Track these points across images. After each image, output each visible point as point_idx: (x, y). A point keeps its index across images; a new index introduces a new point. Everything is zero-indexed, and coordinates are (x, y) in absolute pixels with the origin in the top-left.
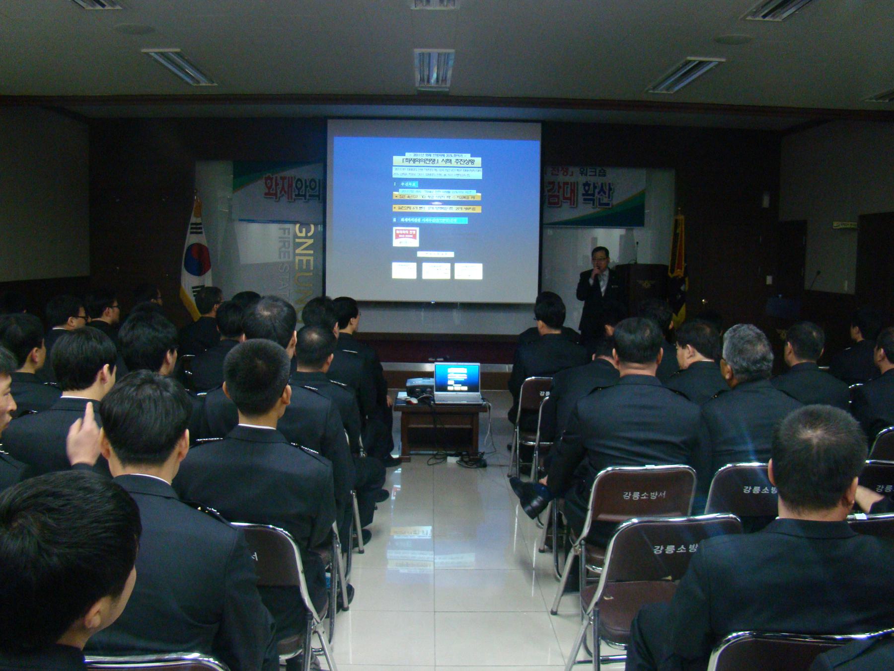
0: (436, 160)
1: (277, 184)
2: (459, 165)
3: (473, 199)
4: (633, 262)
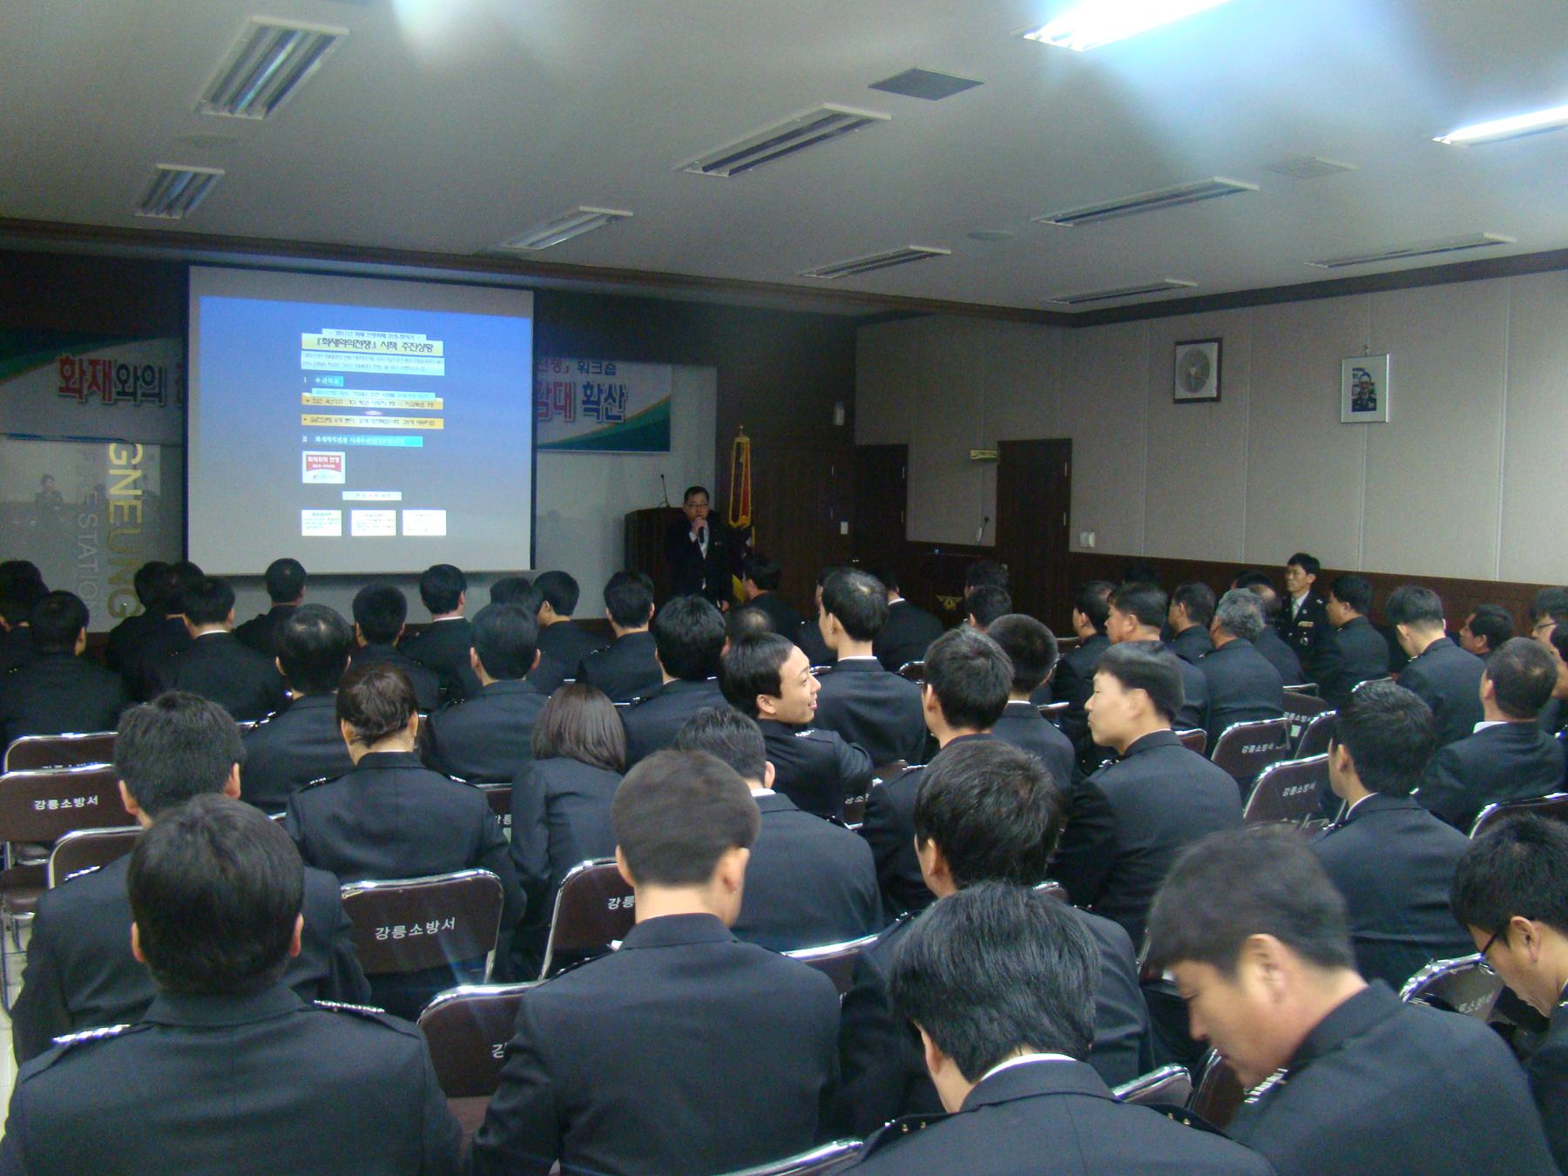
0: (372, 343)
1: (83, 373)
2: (408, 352)
3: (430, 408)
4: (664, 505)
